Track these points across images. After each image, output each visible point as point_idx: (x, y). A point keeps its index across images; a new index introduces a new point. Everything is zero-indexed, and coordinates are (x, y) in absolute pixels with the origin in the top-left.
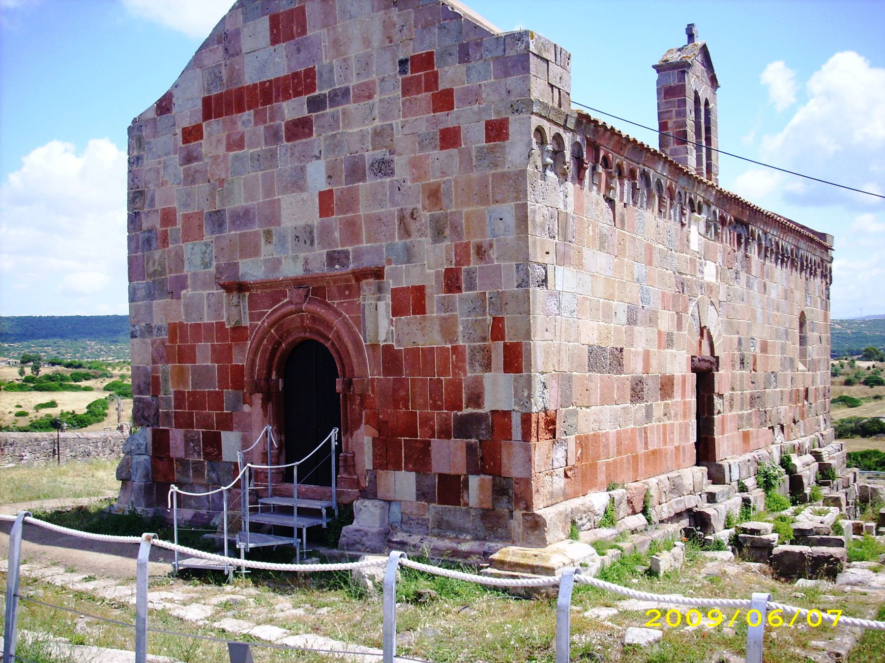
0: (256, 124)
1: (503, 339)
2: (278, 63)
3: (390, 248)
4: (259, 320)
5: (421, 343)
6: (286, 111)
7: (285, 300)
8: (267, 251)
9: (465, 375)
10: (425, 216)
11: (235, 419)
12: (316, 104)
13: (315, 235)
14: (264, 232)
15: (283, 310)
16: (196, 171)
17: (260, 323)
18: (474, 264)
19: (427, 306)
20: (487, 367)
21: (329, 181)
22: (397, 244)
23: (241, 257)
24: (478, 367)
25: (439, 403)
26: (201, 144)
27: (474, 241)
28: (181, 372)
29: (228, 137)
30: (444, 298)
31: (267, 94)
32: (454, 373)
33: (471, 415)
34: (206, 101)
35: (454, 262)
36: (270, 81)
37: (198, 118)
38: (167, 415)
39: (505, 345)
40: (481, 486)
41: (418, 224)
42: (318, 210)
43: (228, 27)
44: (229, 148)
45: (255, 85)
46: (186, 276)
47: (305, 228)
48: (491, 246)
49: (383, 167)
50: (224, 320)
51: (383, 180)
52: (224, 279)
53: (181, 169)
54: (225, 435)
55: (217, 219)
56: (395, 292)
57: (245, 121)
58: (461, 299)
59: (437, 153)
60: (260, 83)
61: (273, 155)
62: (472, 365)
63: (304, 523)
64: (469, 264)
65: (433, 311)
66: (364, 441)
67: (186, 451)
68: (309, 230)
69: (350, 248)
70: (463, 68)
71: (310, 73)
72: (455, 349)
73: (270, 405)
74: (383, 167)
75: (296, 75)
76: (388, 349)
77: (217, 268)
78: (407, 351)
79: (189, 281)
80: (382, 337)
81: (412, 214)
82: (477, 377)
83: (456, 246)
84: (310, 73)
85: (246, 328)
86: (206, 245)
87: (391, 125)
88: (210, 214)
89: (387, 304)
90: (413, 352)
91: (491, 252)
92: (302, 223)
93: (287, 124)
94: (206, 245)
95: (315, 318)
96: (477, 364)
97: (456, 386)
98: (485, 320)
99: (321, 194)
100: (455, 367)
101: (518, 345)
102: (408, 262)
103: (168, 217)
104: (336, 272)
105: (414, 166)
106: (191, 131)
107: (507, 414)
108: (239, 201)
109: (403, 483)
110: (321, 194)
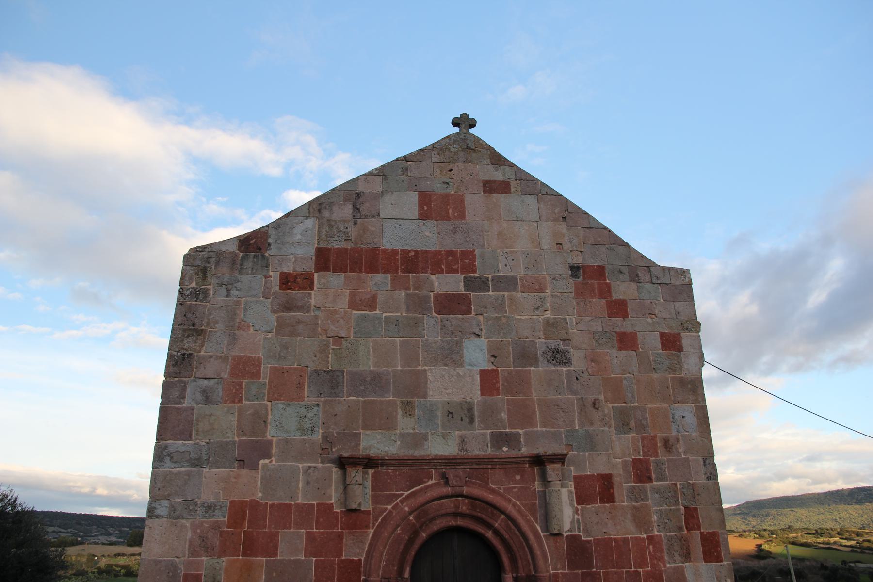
0: (394, 289)
2: (429, 237)
4: (389, 503)
5: (612, 533)
6: (436, 284)
7: (430, 482)
8: (405, 424)
9: (665, 566)
10: (608, 407)
12: (477, 284)
13: (476, 413)
14: (402, 402)
15: (430, 495)
16: (299, 322)
17: (389, 507)
19: (616, 495)
21: (492, 359)
22: (577, 431)
23: (366, 427)
24: (677, 557)
26: (310, 294)
27: (660, 435)
29: (352, 295)
31: (409, 263)
32: (653, 566)
36: (416, 252)
37: (309, 266)
39: (701, 533)
41: (600, 414)
42: (479, 388)
43: (361, 187)
44: (354, 305)
45: (395, 252)
46: (270, 443)
47: (461, 404)
48: (678, 441)
49: (558, 357)
50: (333, 501)
53: (274, 318)
55: (330, 381)
56: (578, 480)
57: (378, 283)
58: (653, 488)
59: (614, 352)
60: (402, 250)
61: (417, 323)
62: (671, 556)
64: (657, 456)
65: (623, 501)
69: (521, 431)
70: (634, 285)
71: (469, 255)
72: (651, 539)
74: (558, 357)
75: (450, 253)
76: (573, 540)
77: (325, 438)
78: (598, 542)
79: (274, 449)
80: (567, 526)
81: (594, 404)
83: (643, 439)
84: (469, 255)
85: (368, 513)
86: (308, 408)
87: (565, 319)
88: (317, 372)
90: (605, 544)
91: (678, 446)
92: (457, 398)
93: (437, 297)
98: (679, 510)
99: (483, 372)
101: (714, 534)
103: (246, 368)
104: (503, 455)
105: (592, 361)
106: (296, 277)
108: (368, 363)
110: (483, 372)
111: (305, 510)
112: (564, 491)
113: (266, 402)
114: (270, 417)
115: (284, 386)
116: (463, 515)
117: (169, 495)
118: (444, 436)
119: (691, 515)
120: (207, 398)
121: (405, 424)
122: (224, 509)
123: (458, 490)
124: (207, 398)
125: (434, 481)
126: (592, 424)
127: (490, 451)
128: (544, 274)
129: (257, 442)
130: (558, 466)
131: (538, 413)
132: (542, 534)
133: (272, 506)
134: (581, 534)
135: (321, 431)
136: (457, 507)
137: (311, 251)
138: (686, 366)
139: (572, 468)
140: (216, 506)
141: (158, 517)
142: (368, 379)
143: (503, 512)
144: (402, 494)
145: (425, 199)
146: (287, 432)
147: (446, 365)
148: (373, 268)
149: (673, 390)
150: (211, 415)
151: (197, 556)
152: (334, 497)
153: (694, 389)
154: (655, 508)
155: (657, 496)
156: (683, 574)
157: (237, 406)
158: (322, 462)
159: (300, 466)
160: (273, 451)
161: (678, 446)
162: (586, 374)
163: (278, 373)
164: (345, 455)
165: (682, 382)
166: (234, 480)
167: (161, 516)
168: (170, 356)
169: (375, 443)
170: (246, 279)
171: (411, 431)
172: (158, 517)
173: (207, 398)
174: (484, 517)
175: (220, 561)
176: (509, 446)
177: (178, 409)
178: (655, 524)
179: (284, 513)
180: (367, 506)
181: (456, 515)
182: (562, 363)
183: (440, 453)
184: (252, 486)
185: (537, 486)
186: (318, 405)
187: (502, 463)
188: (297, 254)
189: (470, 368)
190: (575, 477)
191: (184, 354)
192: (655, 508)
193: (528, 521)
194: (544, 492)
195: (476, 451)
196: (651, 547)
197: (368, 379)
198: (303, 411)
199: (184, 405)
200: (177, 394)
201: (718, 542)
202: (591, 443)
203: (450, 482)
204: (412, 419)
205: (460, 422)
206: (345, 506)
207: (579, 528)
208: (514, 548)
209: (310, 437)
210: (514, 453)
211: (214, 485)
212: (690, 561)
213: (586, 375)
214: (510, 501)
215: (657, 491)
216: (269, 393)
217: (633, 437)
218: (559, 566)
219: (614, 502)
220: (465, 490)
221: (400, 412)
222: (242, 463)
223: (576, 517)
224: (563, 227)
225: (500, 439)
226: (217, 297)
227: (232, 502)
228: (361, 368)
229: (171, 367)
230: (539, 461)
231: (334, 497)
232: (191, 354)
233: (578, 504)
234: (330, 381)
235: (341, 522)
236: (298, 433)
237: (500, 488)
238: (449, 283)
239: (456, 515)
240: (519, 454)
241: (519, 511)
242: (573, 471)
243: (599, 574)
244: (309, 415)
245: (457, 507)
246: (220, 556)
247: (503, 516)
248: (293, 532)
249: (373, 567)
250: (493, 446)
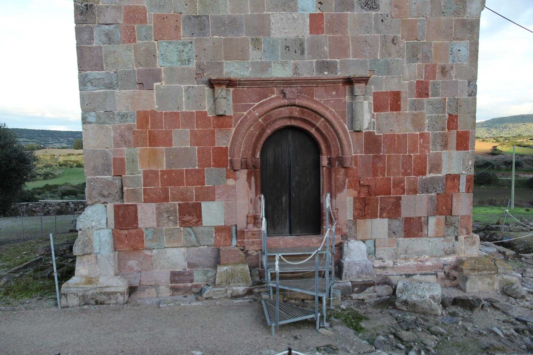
1: (456, 129)
3: (374, 61)
4: (245, 111)
7: (273, 96)
8: (254, 55)
9: (429, 152)
10: (403, 43)
11: (218, 191)
13: (306, 47)
14: (252, 39)
17: (245, 113)
18: (439, 79)
19: (402, 106)
20: (445, 146)
21: (319, 5)
22: (379, 60)
23: (227, 58)
24: (438, 147)
25: (409, 171)
27: (440, 64)
28: (154, 154)
30: (415, 101)
32: (421, 152)
33: (432, 178)
35: (423, 77)
38: (134, 192)
39: (458, 132)
40: (437, 224)
41: (397, 47)
42: (308, 28)
46: (159, 71)
47: (295, 40)
48: (452, 68)
50: (206, 110)
51: (370, 12)
52: (207, 76)
54: (204, 205)
56: (377, 96)
62: (434, 145)
64: (435, 79)
65: (406, 109)
67: (158, 222)
69: (338, 60)
72: (422, 135)
73: (253, 179)
76: (369, 135)
77: (198, 66)
78: (386, 136)
80: (366, 126)
81: (393, 40)
82: (438, 153)
83: (426, 66)
85: (231, 117)
86: (184, 45)
88: (189, 18)
89: (370, 103)
90: (391, 138)
91: (451, 72)
92: (292, 36)
94: (184, 45)
96: (438, 145)
97: (423, 159)
99: (312, 16)
100: (422, 146)
101: (467, 133)
102: (388, 74)
105: (396, 6)
107: (456, 178)
109: (379, 226)
110: (312, 16)
111: (188, 116)
112: (366, 103)
113: (153, 41)
114: (157, 52)
115: (165, 29)
116: (295, 118)
117: (94, 108)
118: (283, 64)
119: (452, 120)
120: (110, 40)
121: (254, 55)
122: (133, 116)
123: (292, 101)
124: (110, 39)
125: (275, 96)
126: (390, 55)
127: (315, 75)
129: (150, 70)
130: (363, 85)
131: (351, 47)
132: (348, 131)
133: (166, 113)
134: (375, 131)
135: (195, 61)
136: (291, 113)
138: (469, 10)
139: (373, 87)
140: (127, 115)
141: (90, 123)
142: (227, 22)
143: (322, 116)
144: (254, 105)
146: (171, 62)
147: (284, 10)
149: (455, 30)
150: (115, 52)
151: (120, 147)
152: (207, 107)
153: (471, 28)
154: (428, 114)
155: (430, 107)
156: (440, 158)
157: (132, 44)
158: (198, 84)
159: (183, 86)
160: (163, 77)
161: (451, 72)
162: (390, 17)
163: (161, 19)
164: (213, 78)
165: (463, 23)
166: (137, 97)
167: (92, 123)
168: (76, 7)
169: (233, 70)
171: (259, 60)
172: (90, 123)
173: (110, 40)
174: (309, 119)
175: (135, 149)
176: (329, 71)
177: (90, 48)
178: (426, 125)
180: (230, 112)
181: (290, 118)
182: (372, 8)
183: (280, 76)
184: (150, 100)
185: (347, 99)
186: (191, 42)
187: (324, 83)
189: (302, 12)
190: (374, 93)
191: (86, 5)
192: (428, 114)
193: (339, 122)
194: (352, 103)
195: (305, 75)
196: (422, 140)
197: (227, 22)
198: (181, 47)
199: (94, 45)
200: (87, 37)
201: (468, 138)
202: (388, 69)
203: (287, 96)
204: (260, 52)
205: (294, 53)
206: (215, 112)
207: (374, 127)
208: (329, 140)
209: (188, 66)
210: (332, 76)
211: (124, 100)
212: (447, 149)
213: (389, 18)
214: (328, 109)
215: (431, 103)
216: (155, 35)
217: (419, 65)
218: (358, 151)
219: (399, 110)
220: (297, 102)
221: (251, 46)
223: (373, 120)
225: (323, 66)
227: (138, 112)
228: (221, 14)
229: (79, 16)
230: (349, 82)
231: (207, 107)
232: (92, 5)
233: (375, 111)
234: (199, 24)
235: (213, 123)
236: (179, 64)
237: (321, 100)
239: (290, 118)
240: (336, 77)
241: (334, 116)
242: (373, 89)
243: (385, 156)
244: (186, 50)
245: (291, 113)
246: (135, 147)
247: (322, 119)
248: (182, 131)
249: (235, 151)
250: (317, 71)
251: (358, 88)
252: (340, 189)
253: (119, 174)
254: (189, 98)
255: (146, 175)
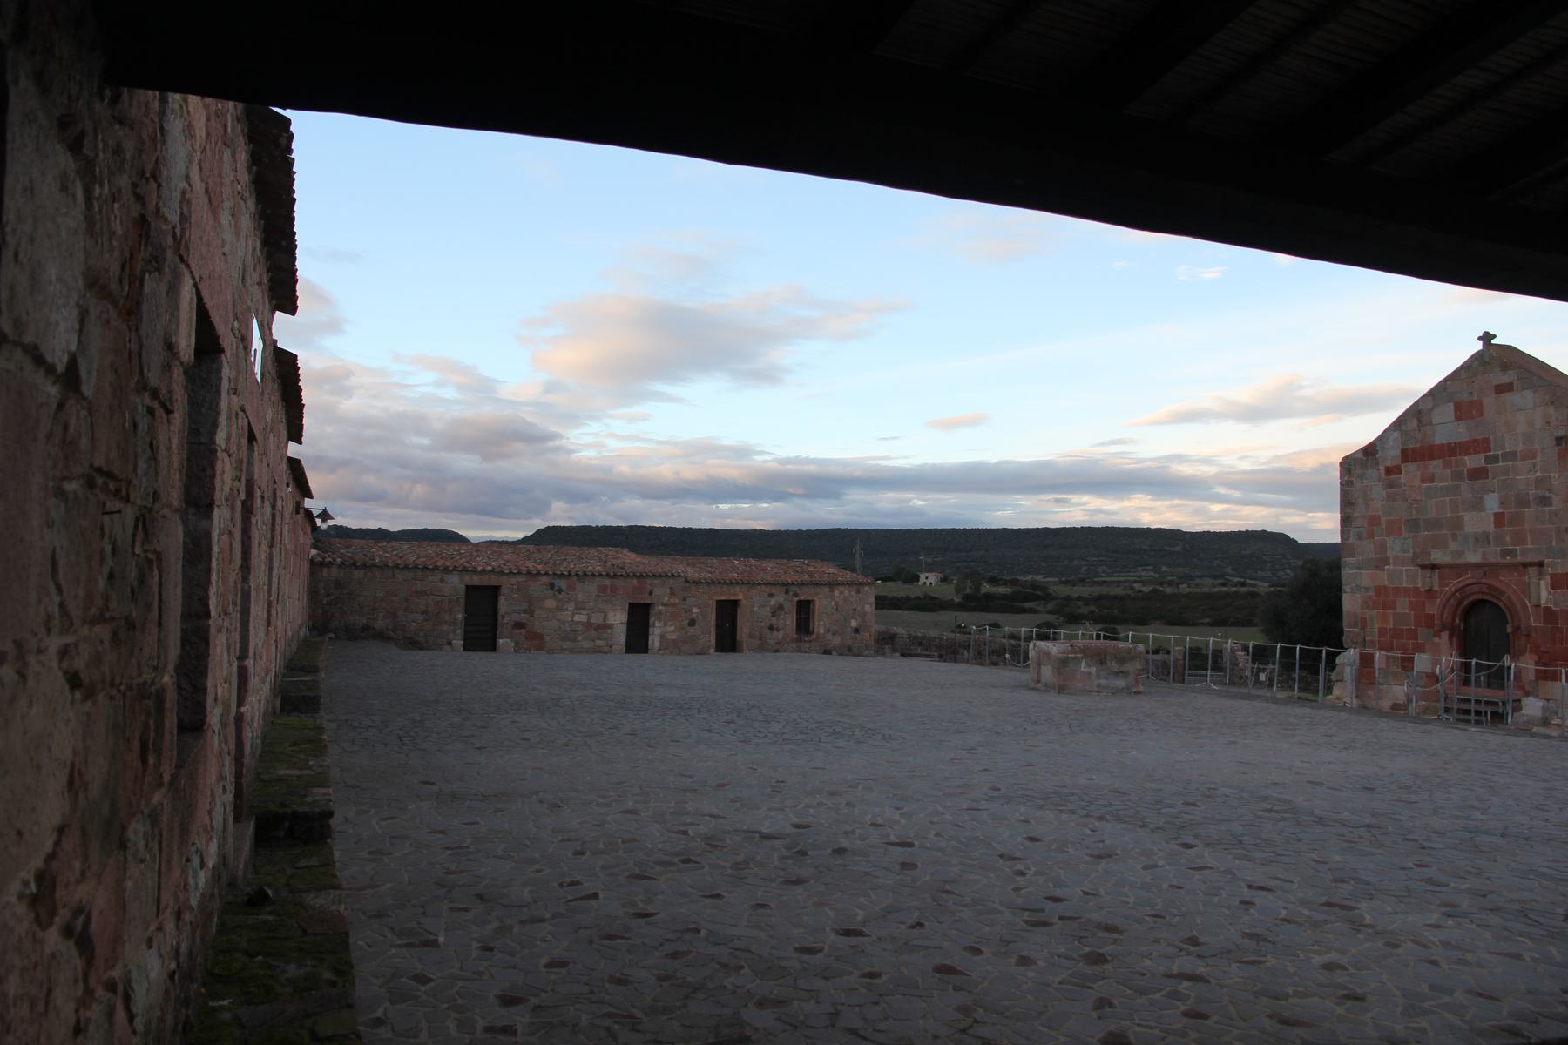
8: (1453, 546)
12: (1495, 459)
31: (1451, 451)
34: (1404, 452)
37: (1398, 461)
44: (1423, 481)
49: (1544, 501)
55: (1414, 525)
56: (1553, 576)
57: (1435, 466)
63: (1489, 709)
66: (1528, 665)
68: (1486, 536)
71: (1486, 440)
74: (1544, 501)
76: (1547, 609)
80: (1543, 601)
84: (1486, 440)
95: (1490, 586)
99: (1496, 515)
103: (1374, 521)
108: (1432, 514)
115: (1393, 529)
120: (1360, 537)
121: (1453, 546)
127: (1499, 560)
128: (1537, 446)
137: (1397, 452)
145: (1458, 407)
148: (1432, 457)
169: (1438, 557)
170: (1369, 472)
173: (1360, 537)
179: (1398, 591)
184: (1384, 579)
188: (1392, 455)
195: (1492, 559)
222: (1377, 567)
224: (1551, 410)
225: (1505, 553)
226: (1357, 484)
230: (1525, 565)
234: (1414, 525)
238: (1474, 461)
242: (1550, 571)
251: (1532, 571)
252: (1523, 653)
253: (1363, 629)
254: (1408, 577)
255: (1380, 630)
